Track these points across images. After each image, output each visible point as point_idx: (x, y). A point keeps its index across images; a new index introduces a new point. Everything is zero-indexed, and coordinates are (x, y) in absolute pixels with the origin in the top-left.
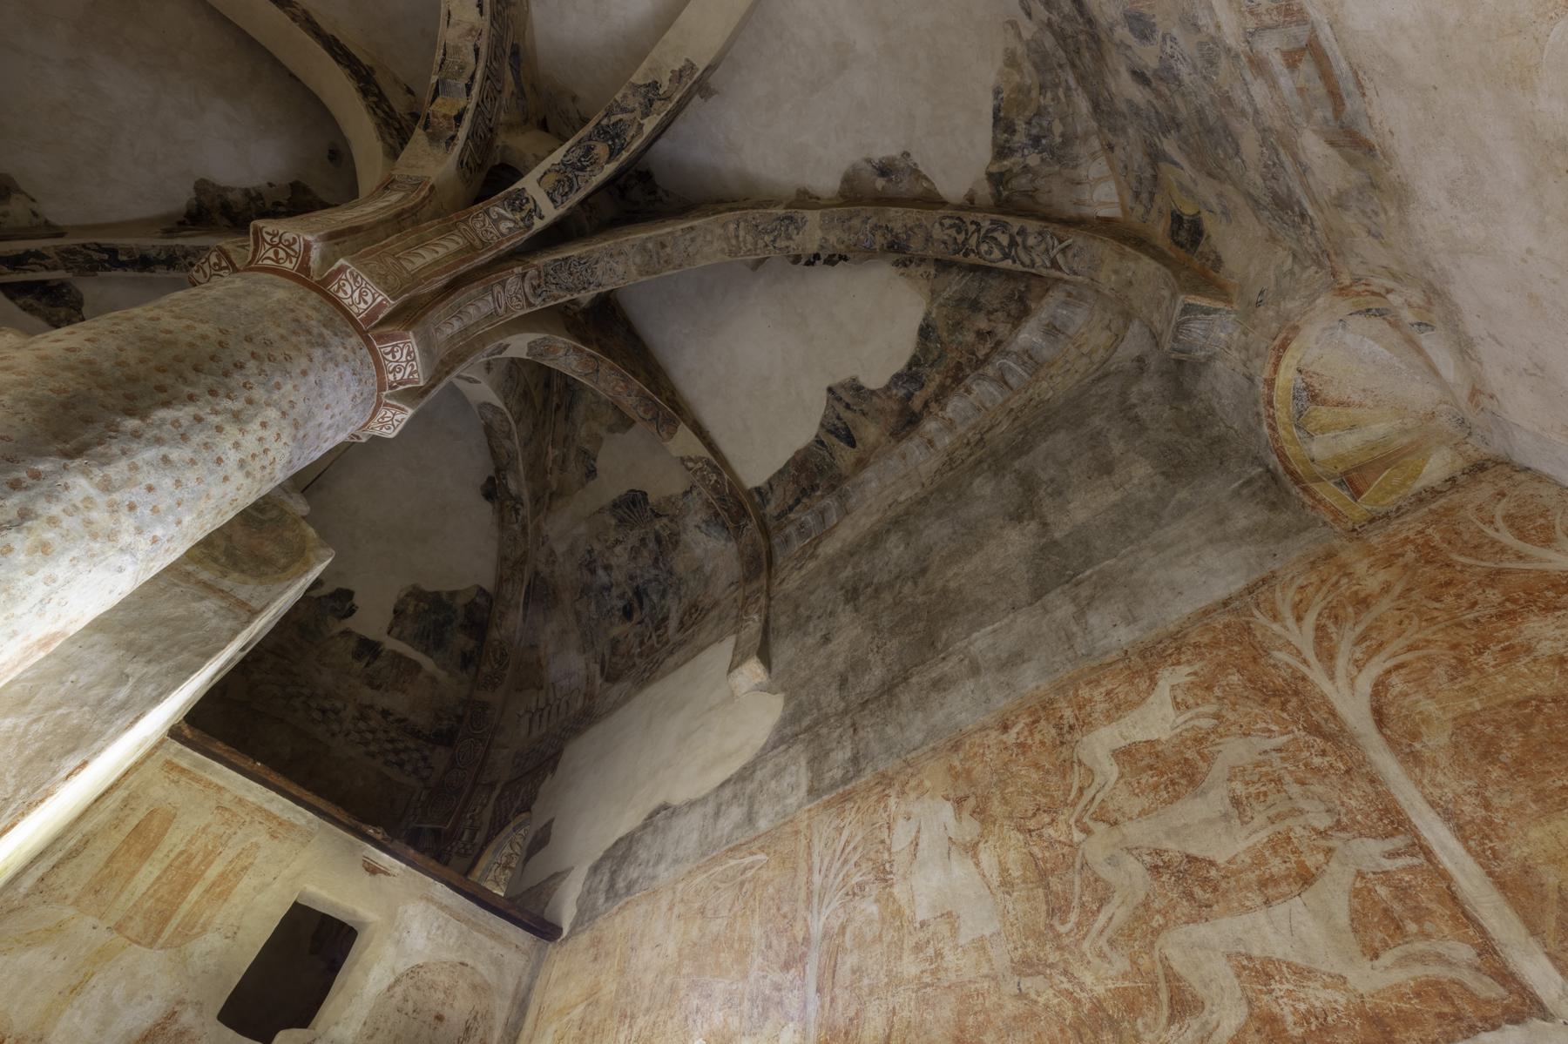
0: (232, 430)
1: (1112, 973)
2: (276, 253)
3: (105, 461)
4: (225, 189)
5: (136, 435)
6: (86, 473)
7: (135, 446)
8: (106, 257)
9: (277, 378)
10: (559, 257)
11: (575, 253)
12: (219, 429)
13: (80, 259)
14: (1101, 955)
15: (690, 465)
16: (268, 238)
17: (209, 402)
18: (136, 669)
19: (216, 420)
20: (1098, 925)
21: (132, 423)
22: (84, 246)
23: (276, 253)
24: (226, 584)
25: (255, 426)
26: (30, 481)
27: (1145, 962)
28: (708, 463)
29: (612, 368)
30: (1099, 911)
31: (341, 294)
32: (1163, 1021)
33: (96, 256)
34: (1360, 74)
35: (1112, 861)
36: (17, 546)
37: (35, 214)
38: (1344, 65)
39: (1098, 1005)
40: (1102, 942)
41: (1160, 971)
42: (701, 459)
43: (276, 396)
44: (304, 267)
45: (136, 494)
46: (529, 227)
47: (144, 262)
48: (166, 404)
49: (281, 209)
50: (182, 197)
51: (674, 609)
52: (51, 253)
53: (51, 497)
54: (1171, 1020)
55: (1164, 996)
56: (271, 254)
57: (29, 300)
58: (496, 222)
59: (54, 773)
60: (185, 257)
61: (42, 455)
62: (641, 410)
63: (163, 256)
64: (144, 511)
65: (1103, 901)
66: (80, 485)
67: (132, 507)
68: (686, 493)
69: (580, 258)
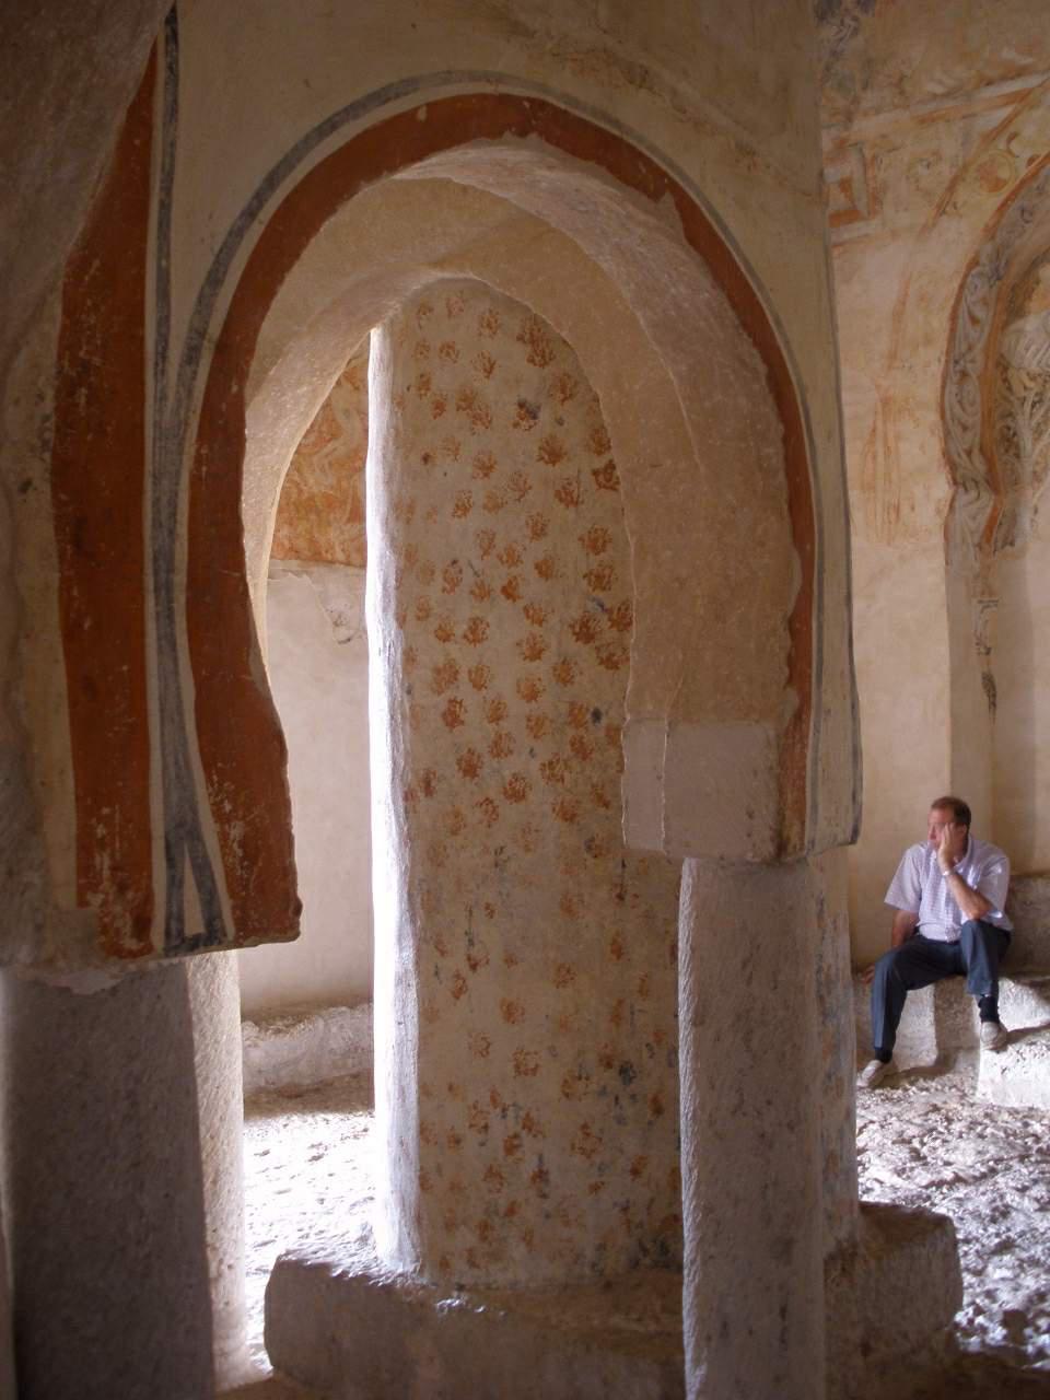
1: (326, 483)
14: (323, 470)
20: (326, 450)
27: (344, 484)
30: (329, 441)
32: (345, 519)
34: (841, 249)
35: (347, 412)
38: (846, 236)
39: (312, 498)
40: (326, 462)
41: (351, 492)
54: (349, 520)
55: (349, 507)
65: (334, 437)
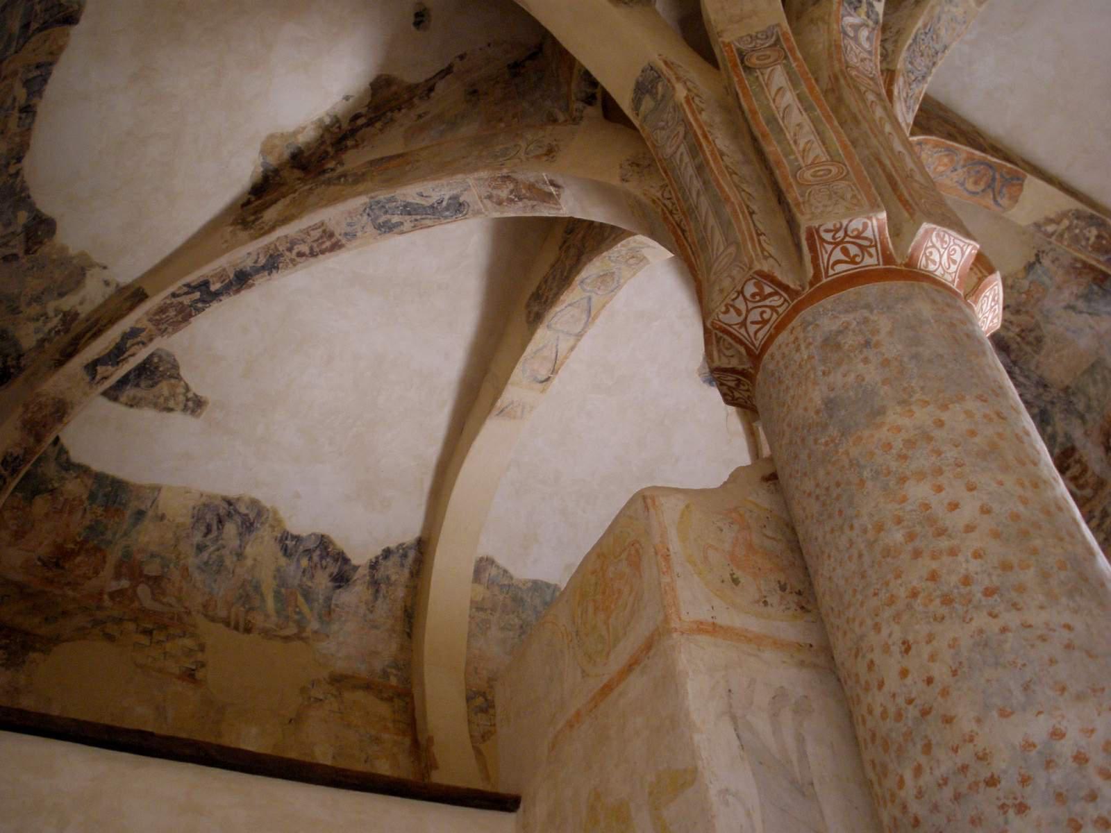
2: (845, 251)
4: (295, 134)
8: (197, 295)
10: (910, 41)
11: (920, 24)
13: (172, 313)
15: (1050, 228)
16: (828, 237)
22: (174, 295)
23: (845, 251)
28: (1078, 215)
29: (936, 145)
31: (932, 267)
33: (186, 300)
37: (107, 283)
42: (1064, 215)
44: (888, 258)
46: (877, 22)
47: (242, 280)
49: (360, 122)
50: (244, 169)
51: (1077, 433)
52: (145, 323)
56: (838, 254)
57: (130, 392)
58: (856, 39)
60: (290, 250)
62: (971, 187)
63: (262, 261)
68: (1030, 267)
69: (925, 26)
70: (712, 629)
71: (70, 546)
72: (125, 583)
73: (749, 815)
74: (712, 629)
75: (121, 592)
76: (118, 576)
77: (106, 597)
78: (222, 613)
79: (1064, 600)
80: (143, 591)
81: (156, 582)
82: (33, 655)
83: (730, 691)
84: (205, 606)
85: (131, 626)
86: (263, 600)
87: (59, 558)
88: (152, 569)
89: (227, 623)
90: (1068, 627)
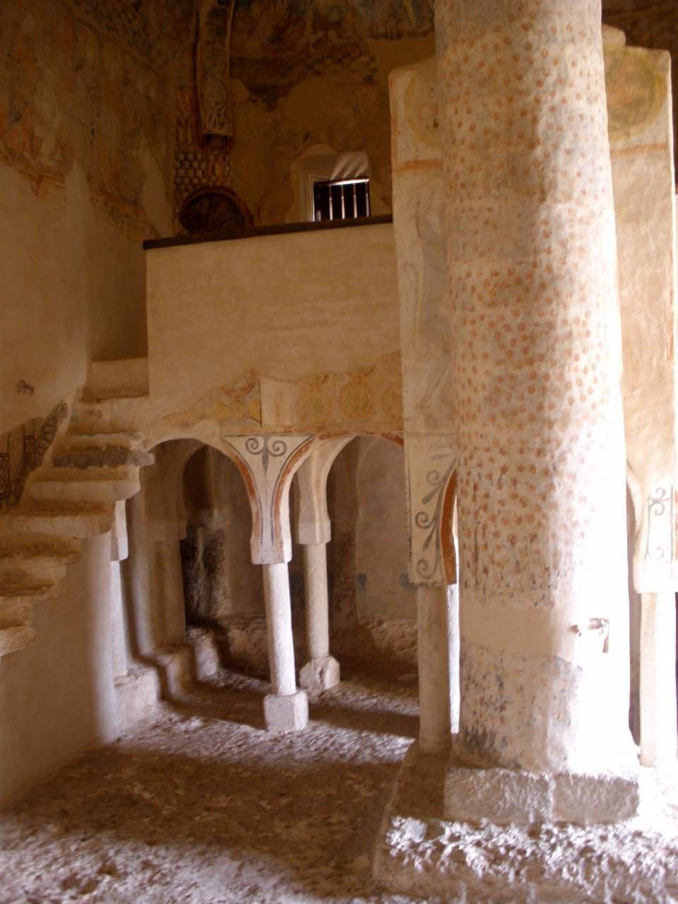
0: (569, 93)
3: (553, 184)
5: (547, 156)
6: (556, 201)
7: (552, 163)
9: (549, 26)
12: (564, 101)
17: (544, 92)
18: (645, 229)
19: (557, 99)
21: (539, 151)
24: (634, 140)
25: (573, 73)
26: (548, 228)
36: (576, 261)
43: (559, 37)
45: (579, 184)
48: (535, 120)
53: (560, 227)
59: (665, 304)
61: (536, 211)
64: (589, 187)
66: (561, 209)
67: (584, 193)
70: (415, 165)
71: (282, 24)
72: (320, 34)
73: (416, 274)
74: (415, 165)
75: (319, 40)
76: (315, 31)
77: (311, 48)
78: (381, 31)
79: (493, 191)
80: (332, 34)
81: (338, 25)
82: (281, 100)
83: (419, 202)
84: (371, 30)
85: (329, 61)
86: (406, 11)
87: (278, 35)
88: (334, 17)
89: (385, 36)
90: (490, 210)
